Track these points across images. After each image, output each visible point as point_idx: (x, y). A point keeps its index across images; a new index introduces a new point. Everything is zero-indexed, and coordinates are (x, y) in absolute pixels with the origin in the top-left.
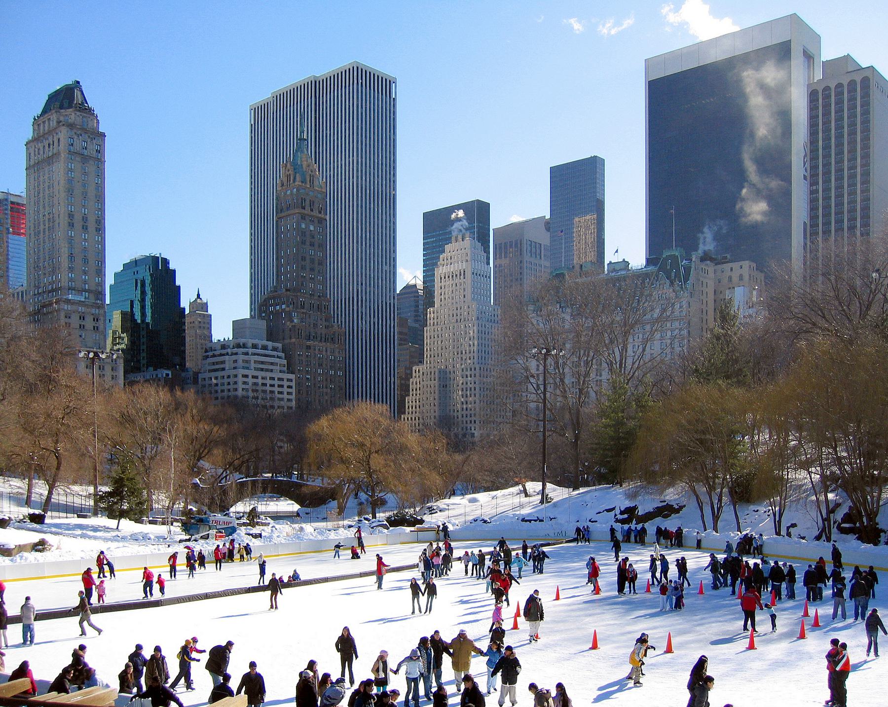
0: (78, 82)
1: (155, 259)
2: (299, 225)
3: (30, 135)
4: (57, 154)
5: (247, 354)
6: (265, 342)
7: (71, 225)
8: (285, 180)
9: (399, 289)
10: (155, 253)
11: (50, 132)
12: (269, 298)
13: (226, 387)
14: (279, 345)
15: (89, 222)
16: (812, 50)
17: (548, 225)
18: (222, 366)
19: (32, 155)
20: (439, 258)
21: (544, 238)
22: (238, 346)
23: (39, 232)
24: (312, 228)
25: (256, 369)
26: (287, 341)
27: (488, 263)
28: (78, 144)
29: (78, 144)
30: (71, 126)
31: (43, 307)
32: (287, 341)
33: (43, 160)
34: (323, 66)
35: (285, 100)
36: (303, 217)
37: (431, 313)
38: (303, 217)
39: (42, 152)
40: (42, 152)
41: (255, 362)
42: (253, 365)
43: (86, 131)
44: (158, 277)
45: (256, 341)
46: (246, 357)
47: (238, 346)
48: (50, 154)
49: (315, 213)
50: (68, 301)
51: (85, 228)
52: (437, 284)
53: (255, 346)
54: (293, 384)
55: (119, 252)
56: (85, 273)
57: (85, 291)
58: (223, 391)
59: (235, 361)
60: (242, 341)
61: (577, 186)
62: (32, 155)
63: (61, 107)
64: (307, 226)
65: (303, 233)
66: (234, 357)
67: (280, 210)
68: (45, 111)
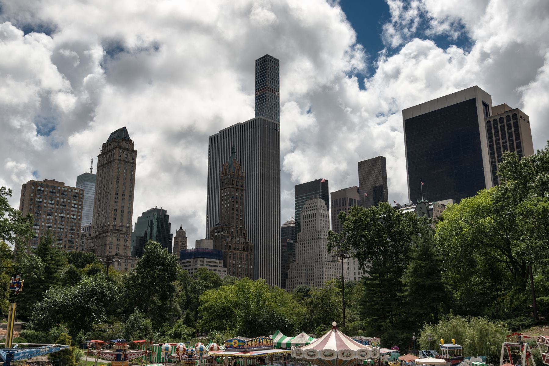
3: (100, 152)
4: (113, 161)
8: (224, 171)
9: (282, 223)
11: (110, 151)
16: (487, 102)
17: (358, 190)
18: (189, 264)
20: (302, 208)
27: (328, 210)
28: (123, 156)
31: (99, 234)
33: (105, 164)
39: (105, 160)
42: (205, 263)
43: (127, 150)
52: (302, 221)
55: (140, 208)
65: (233, 197)
67: (222, 186)
68: (108, 141)
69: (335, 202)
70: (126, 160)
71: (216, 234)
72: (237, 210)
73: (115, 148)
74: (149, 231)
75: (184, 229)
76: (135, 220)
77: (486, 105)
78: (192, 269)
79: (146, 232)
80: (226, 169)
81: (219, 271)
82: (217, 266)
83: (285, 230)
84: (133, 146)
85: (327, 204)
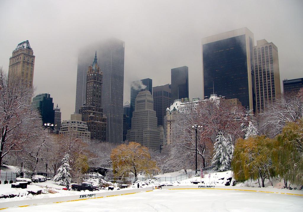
0: (28, 41)
1: (46, 94)
2: (93, 85)
3: (11, 56)
8: (90, 71)
11: (17, 56)
14: (86, 122)
18: (67, 129)
19: (11, 62)
20: (136, 96)
22: (72, 122)
24: (98, 86)
26: (88, 121)
28: (26, 59)
29: (26, 59)
32: (88, 121)
36: (95, 82)
38: (95, 82)
39: (14, 61)
41: (78, 128)
45: (78, 121)
47: (72, 122)
48: (17, 62)
49: (99, 81)
54: (90, 135)
60: (73, 121)
64: (96, 85)
65: (95, 88)
67: (88, 80)
69: (155, 93)
70: (29, 62)
71: (84, 111)
72: (97, 96)
81: (85, 134)
82: (84, 131)
83: (127, 109)
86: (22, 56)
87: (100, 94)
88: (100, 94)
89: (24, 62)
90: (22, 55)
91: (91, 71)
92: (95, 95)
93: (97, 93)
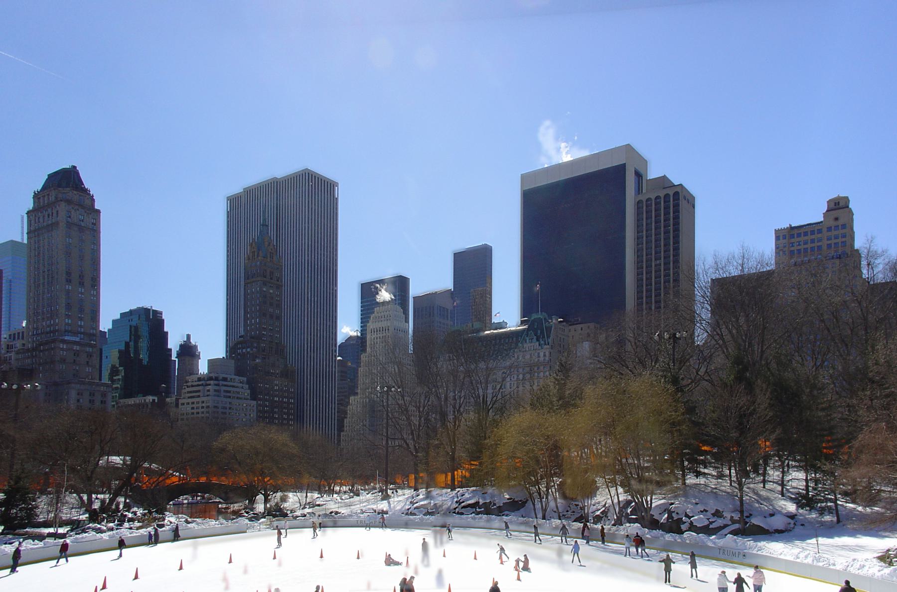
3: (30, 205)
4: (56, 224)
5: (218, 385)
6: (233, 377)
7: (69, 281)
9: (340, 339)
10: (148, 306)
12: (236, 344)
13: (200, 410)
14: (245, 379)
15: (87, 277)
16: (642, 171)
17: (450, 294)
19: (33, 222)
21: (449, 305)
22: (211, 379)
23: (39, 285)
25: (225, 397)
27: (407, 321)
30: (69, 202)
31: (40, 345)
34: (282, 168)
35: (250, 192)
36: (265, 284)
37: (364, 357)
39: (41, 220)
40: (41, 220)
41: (225, 391)
42: (223, 394)
43: (82, 206)
44: (147, 325)
46: (217, 388)
48: (50, 222)
50: (64, 342)
51: (82, 284)
52: (368, 337)
53: (225, 379)
56: (81, 319)
57: (81, 333)
58: (198, 413)
59: (209, 391)
60: (213, 375)
61: (473, 266)
62: (33, 222)
63: (59, 186)
66: (208, 388)
67: (247, 277)
73: (57, 200)
74: (132, 344)
75: (193, 342)
76: (105, 325)
77: (639, 175)
78: (203, 402)
79: (127, 344)
80: (254, 252)
84: (93, 200)
85: (406, 312)
86: (62, 208)
87: (278, 312)
88: (278, 312)
89: (69, 225)
90: (63, 204)
91: (254, 255)
92: (264, 315)
93: (271, 310)
